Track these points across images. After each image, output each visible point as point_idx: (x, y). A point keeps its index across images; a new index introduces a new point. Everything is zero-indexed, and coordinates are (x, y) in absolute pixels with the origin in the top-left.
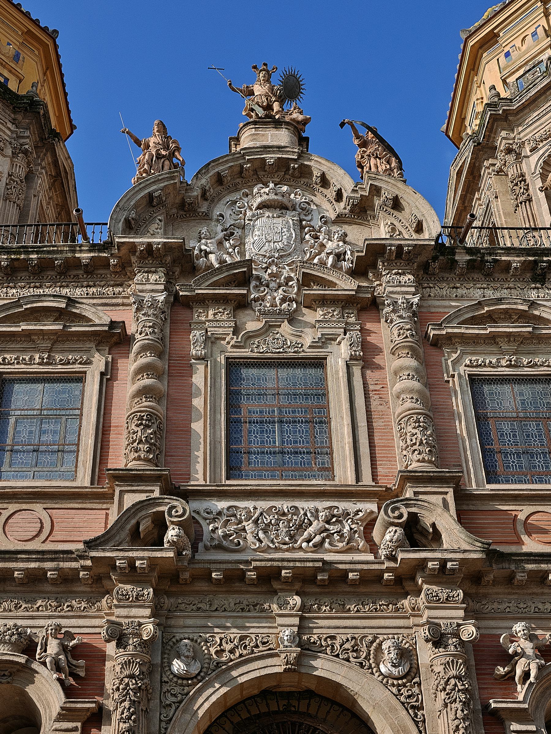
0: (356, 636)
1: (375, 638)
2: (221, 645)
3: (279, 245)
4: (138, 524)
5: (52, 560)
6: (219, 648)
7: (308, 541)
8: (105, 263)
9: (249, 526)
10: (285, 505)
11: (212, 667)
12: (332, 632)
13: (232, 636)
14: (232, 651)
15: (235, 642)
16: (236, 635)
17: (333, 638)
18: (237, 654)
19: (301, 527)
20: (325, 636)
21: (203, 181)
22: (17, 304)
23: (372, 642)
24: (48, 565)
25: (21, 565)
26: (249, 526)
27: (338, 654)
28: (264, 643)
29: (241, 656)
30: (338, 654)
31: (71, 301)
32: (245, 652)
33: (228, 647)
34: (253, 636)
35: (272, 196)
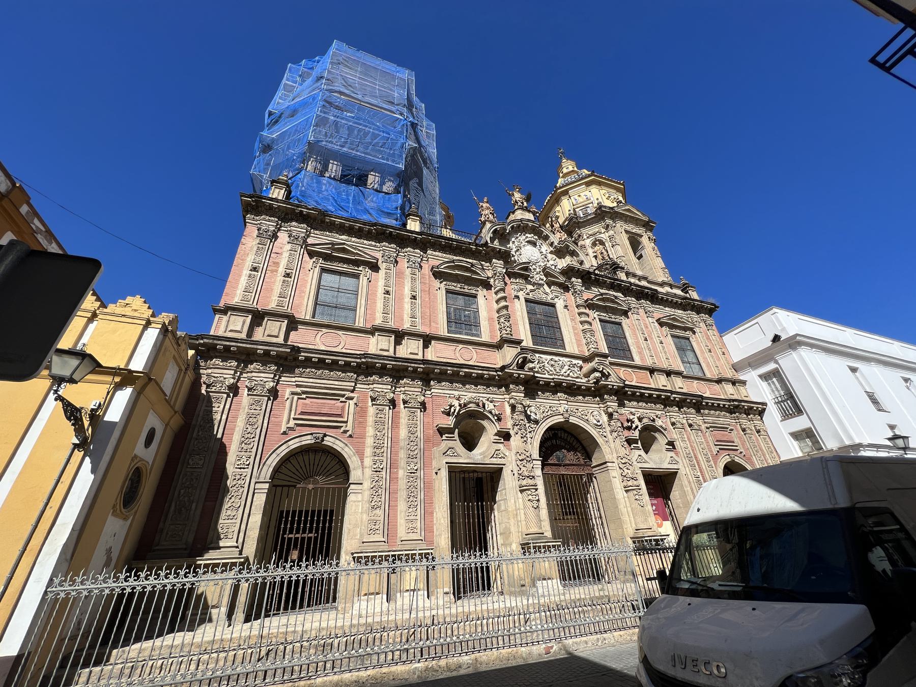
3: (536, 258)
4: (518, 361)
5: (487, 371)
7: (565, 372)
8: (480, 252)
9: (547, 365)
10: (556, 358)
19: (562, 367)
21: (509, 227)
22: (453, 261)
24: (485, 372)
25: (475, 371)
26: (547, 365)
31: (472, 265)
33: (546, 410)
35: (532, 239)
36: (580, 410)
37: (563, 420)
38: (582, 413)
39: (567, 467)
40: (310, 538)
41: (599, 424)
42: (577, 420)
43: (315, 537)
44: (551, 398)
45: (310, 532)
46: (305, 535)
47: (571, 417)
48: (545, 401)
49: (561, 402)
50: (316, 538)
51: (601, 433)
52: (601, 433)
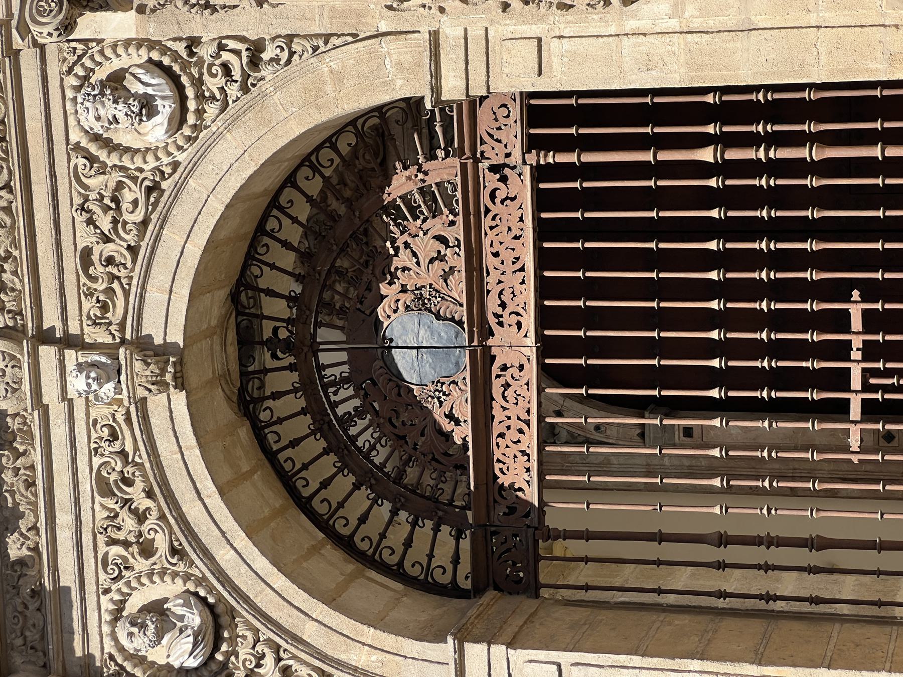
0: (78, 200)
1: (77, 147)
2: (126, 544)
6: (135, 549)
11: (181, 567)
12: (71, 262)
13: (101, 514)
14: (141, 517)
15: (117, 507)
16: (97, 507)
17: (86, 256)
18: (149, 503)
20: (83, 279)
23: (91, 159)
27: (129, 248)
28: (114, 436)
29: (150, 494)
30: (129, 248)
32: (139, 484)
33: (129, 522)
34: (97, 461)
36: (86, 237)
37: (179, 400)
38: (105, 223)
39: (492, 304)
40: (871, 321)
41: (166, 108)
42: (160, 276)
43: (864, 300)
44: (37, 457)
45: (841, 321)
46: (857, 342)
47: (153, 328)
48: (64, 518)
49: (50, 395)
50: (870, 291)
51: (233, 91)
52: (233, 91)
